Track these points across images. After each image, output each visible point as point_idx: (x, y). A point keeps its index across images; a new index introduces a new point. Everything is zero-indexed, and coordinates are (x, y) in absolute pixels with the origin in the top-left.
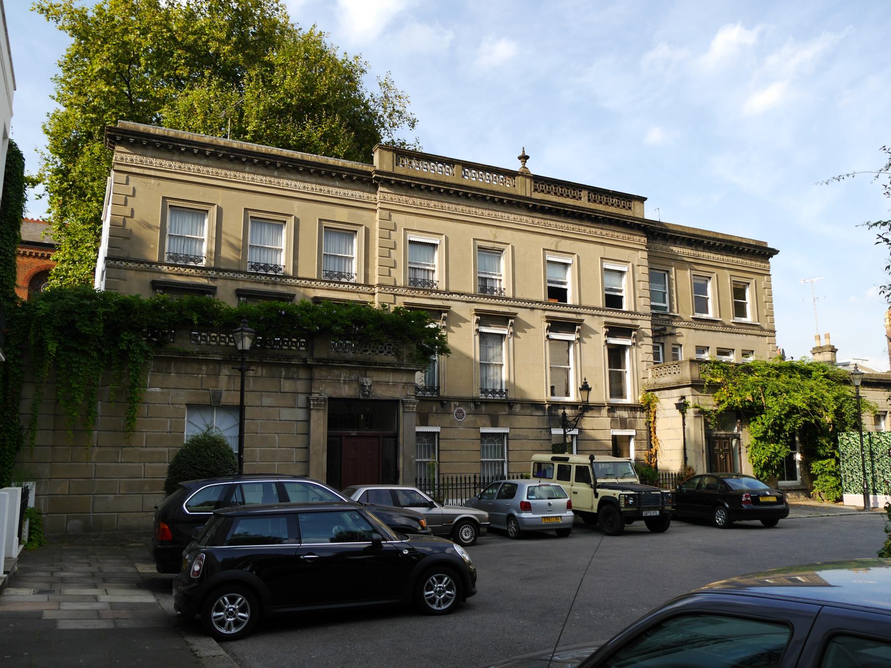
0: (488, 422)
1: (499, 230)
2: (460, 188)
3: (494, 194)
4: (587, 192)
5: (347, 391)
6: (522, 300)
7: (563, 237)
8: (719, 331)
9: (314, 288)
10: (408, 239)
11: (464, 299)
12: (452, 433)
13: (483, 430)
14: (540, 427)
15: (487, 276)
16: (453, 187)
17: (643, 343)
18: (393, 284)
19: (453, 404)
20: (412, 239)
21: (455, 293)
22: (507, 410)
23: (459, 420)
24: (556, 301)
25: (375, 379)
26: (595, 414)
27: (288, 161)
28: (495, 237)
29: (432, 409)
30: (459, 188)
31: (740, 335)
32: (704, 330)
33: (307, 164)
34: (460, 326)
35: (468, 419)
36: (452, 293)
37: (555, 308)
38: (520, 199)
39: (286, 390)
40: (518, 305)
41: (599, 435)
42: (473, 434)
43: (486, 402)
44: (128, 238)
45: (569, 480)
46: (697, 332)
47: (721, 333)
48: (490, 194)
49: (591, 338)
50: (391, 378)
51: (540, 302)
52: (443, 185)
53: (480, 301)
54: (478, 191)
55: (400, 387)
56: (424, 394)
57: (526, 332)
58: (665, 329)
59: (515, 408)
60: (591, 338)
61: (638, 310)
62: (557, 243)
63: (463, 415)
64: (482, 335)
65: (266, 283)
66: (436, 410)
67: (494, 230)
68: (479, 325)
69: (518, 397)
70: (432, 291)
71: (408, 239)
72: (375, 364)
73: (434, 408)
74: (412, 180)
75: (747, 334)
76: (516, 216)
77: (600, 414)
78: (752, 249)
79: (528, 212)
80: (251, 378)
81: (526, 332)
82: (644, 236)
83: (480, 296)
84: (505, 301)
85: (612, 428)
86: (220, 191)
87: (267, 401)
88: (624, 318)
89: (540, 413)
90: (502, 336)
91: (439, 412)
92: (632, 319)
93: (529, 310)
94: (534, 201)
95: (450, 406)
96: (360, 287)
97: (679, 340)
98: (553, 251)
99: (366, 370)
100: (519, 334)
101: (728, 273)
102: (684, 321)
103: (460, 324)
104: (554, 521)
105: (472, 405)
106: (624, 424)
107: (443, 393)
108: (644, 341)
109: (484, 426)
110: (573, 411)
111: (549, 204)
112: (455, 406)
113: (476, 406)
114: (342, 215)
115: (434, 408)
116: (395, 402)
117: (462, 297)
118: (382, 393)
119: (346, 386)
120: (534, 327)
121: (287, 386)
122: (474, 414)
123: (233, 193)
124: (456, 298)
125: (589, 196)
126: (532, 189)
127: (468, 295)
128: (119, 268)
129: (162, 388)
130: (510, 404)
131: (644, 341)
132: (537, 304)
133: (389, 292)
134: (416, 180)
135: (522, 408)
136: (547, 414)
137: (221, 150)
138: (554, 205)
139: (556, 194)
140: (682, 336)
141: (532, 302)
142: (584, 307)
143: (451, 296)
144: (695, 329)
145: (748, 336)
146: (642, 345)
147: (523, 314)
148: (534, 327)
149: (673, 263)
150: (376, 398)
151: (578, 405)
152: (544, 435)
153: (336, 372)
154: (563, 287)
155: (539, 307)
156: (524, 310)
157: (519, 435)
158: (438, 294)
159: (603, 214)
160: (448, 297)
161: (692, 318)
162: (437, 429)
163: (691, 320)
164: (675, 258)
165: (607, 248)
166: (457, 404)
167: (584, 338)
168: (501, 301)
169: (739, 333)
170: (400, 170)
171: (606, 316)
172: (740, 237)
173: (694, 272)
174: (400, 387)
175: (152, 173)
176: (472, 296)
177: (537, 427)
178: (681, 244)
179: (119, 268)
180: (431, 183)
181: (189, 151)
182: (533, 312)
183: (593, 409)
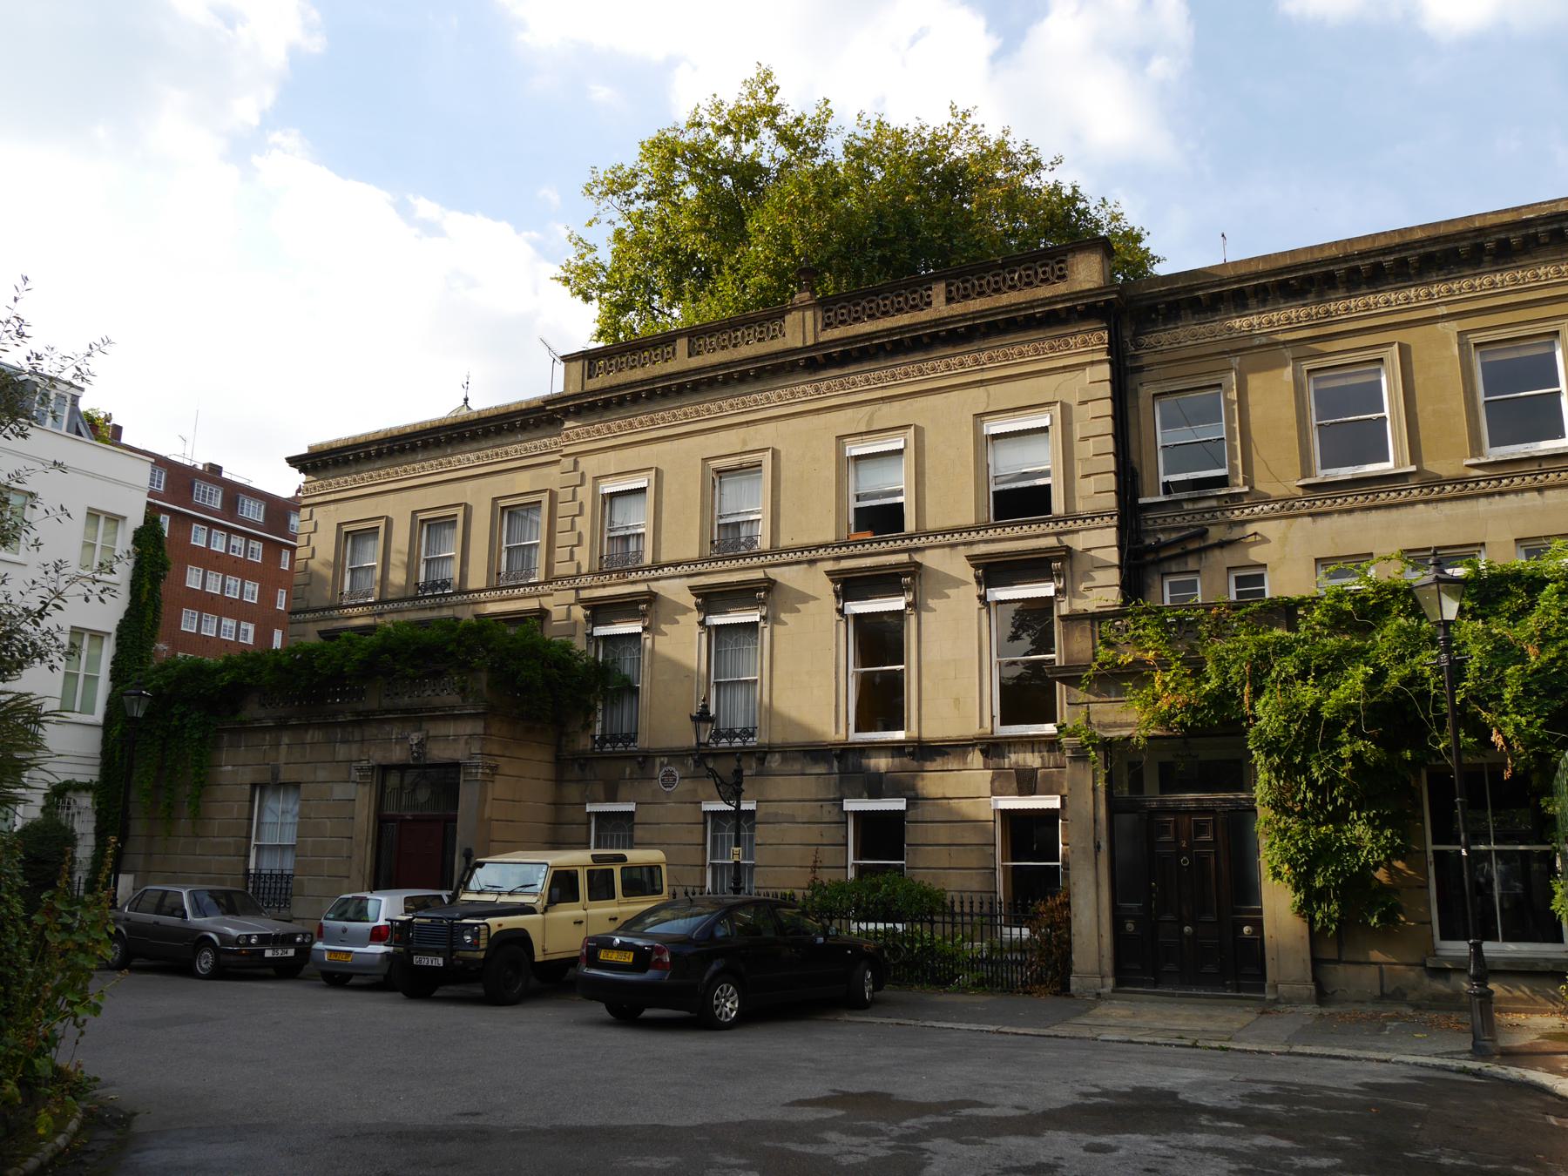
1: (752, 429)
2: (670, 380)
4: (943, 285)
5: (397, 755)
6: (794, 550)
7: (882, 399)
8: (1413, 503)
9: (485, 602)
10: (601, 492)
13: (707, 807)
14: (820, 797)
15: (739, 519)
16: (659, 382)
17: (1089, 584)
18: (574, 572)
19: (658, 761)
20: (607, 491)
22: (754, 765)
23: (668, 789)
24: (868, 535)
25: (432, 733)
27: (450, 430)
28: (744, 443)
30: (667, 380)
31: (1512, 497)
32: (1350, 511)
33: (472, 425)
35: (681, 787)
36: (661, 567)
37: (868, 548)
38: (777, 358)
39: (340, 759)
41: (968, 808)
44: (308, 584)
45: (577, 900)
46: (1324, 523)
47: (1421, 507)
48: (721, 369)
49: (949, 597)
50: (450, 729)
51: (825, 546)
52: (643, 385)
53: (710, 569)
55: (462, 742)
56: (730, 743)
58: (1202, 533)
59: (770, 762)
60: (949, 597)
61: (1081, 507)
62: (872, 414)
63: (675, 780)
64: (710, 630)
65: (431, 609)
66: (631, 773)
67: (743, 431)
68: (708, 613)
69: (778, 739)
70: (630, 571)
71: (601, 492)
72: (436, 709)
75: (1540, 490)
77: (965, 763)
78: (1464, 245)
79: (810, 374)
80: (308, 746)
81: (798, 611)
82: (1101, 329)
83: (716, 560)
84: (755, 559)
85: (994, 793)
86: (391, 496)
87: (322, 775)
88: (1038, 536)
89: (821, 769)
90: (753, 626)
91: (635, 776)
92: (1058, 534)
93: (806, 566)
96: (540, 588)
97: (1256, 554)
98: (861, 434)
99: (421, 720)
100: (783, 616)
101: (1453, 327)
102: (1267, 503)
103: (677, 617)
104: (342, 958)
105: (691, 761)
106: (1027, 783)
107: (643, 742)
108: (1093, 579)
109: (710, 799)
110: (897, 760)
111: (837, 346)
112: (662, 765)
113: (697, 763)
114: (522, 482)
116: (455, 766)
118: (440, 753)
119: (398, 747)
121: (342, 752)
122: (694, 777)
123: (405, 494)
124: (670, 574)
125: (950, 292)
126: (819, 327)
127: (688, 563)
128: (299, 622)
129: (234, 766)
130: (761, 754)
131: (1093, 579)
132: (821, 551)
133: (568, 586)
134: (601, 394)
135: (784, 760)
137: (383, 444)
138: (850, 343)
140: (1265, 540)
141: (809, 548)
142: (927, 534)
143: (660, 571)
144: (1310, 515)
145: (1549, 493)
146: (1090, 589)
147: (782, 575)
149: (1235, 361)
150: (432, 762)
151: (904, 747)
152: (828, 812)
153: (387, 728)
154: (899, 499)
156: (795, 568)
157: (776, 815)
159: (966, 320)
160: (657, 575)
161: (1303, 487)
162: (631, 807)
163: (1300, 492)
164: (1248, 344)
165: (992, 388)
166: (666, 760)
167: (929, 601)
169: (1501, 494)
170: (594, 384)
171: (986, 542)
172: (1506, 211)
173: (1307, 365)
174: (462, 742)
175: (332, 497)
177: (814, 797)
178: (1264, 302)
179: (299, 622)
181: (357, 459)
182: (814, 568)
183: (948, 754)
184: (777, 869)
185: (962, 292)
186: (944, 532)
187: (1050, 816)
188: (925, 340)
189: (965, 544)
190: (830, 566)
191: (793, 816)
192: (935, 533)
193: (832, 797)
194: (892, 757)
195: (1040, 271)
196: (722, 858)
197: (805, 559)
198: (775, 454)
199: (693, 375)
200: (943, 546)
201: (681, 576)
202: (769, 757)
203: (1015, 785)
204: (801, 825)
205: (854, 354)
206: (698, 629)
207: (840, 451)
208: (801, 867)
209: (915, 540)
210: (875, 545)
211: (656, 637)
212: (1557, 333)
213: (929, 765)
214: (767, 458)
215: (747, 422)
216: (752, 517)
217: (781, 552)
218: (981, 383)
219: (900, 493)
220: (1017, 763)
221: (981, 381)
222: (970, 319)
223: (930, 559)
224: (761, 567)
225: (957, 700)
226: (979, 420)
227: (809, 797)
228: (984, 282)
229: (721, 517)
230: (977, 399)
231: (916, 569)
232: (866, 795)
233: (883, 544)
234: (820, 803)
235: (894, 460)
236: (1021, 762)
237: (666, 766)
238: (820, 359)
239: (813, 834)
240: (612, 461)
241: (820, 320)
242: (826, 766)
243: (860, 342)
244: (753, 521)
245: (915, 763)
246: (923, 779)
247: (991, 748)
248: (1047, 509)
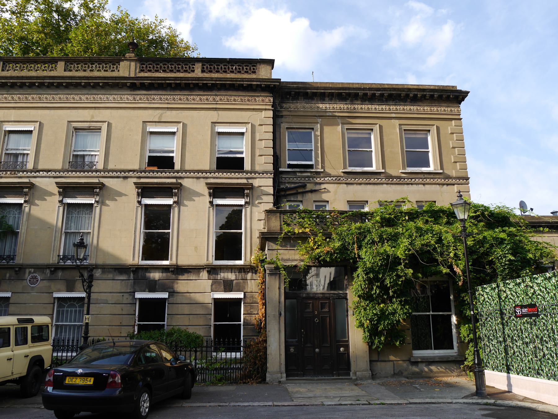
0: (64, 287)
1: (97, 111)
2: (54, 79)
3: (88, 80)
4: (201, 64)
6: (116, 171)
7: (167, 108)
8: (382, 184)
10: (4, 129)
11: (51, 175)
12: (24, 298)
13: (56, 295)
14: (123, 291)
15: (85, 153)
16: (47, 79)
17: (260, 201)
19: (27, 271)
20: (8, 129)
21: (42, 171)
23: (32, 286)
24: (155, 168)
26: (193, 277)
28: (93, 117)
29: (6, 276)
31: (415, 186)
32: (360, 184)
34: (46, 200)
35: (41, 284)
36: (39, 171)
38: (116, 80)
40: (108, 175)
41: (199, 298)
42: (45, 298)
43: (64, 268)
46: (351, 187)
47: (385, 185)
48: (84, 80)
49: (195, 201)
51: (134, 171)
52: (37, 79)
53: (68, 175)
54: (72, 79)
57: (116, 200)
58: (304, 186)
60: (195, 201)
61: (257, 168)
63: (37, 281)
67: (92, 111)
68: (65, 197)
69: (100, 262)
70: (19, 171)
71: (4, 129)
73: (8, 275)
74: (7, 79)
75: (424, 184)
76: (116, 97)
77: (199, 277)
79: (131, 91)
81: (116, 200)
82: (270, 96)
83: (72, 171)
84: (94, 173)
85: (212, 291)
88: (238, 178)
89: (124, 277)
90: (91, 205)
91: (12, 278)
92: (247, 178)
93: (122, 179)
94: (131, 80)
95: (25, 273)
97: (325, 197)
98: (155, 122)
100: (107, 202)
101: (397, 122)
102: (330, 177)
103: (46, 197)
105: (48, 271)
106: (228, 286)
107: (19, 260)
108: (262, 199)
109: (59, 291)
110: (164, 274)
111: (148, 80)
112: (30, 273)
113: (52, 273)
115: (8, 275)
117: (49, 173)
120: (126, 195)
122: (49, 280)
124: (43, 175)
125: (203, 68)
126: (138, 71)
127: (55, 171)
131: (262, 199)
132: (131, 173)
135: (103, 272)
136: (132, 279)
139: (163, 71)
140: (328, 191)
141: (125, 171)
142: (186, 172)
143: (37, 173)
144: (346, 184)
145: (426, 186)
146: (261, 203)
148: (126, 195)
149: (319, 120)
152: (127, 298)
154: (171, 155)
155: (133, 175)
156: (116, 179)
157: (97, 299)
158: (25, 173)
159: (212, 81)
160: (35, 175)
161: (344, 172)
162: (8, 295)
163: (342, 174)
164: (324, 114)
165: (220, 112)
166: (32, 270)
168: (86, 173)
169: (412, 184)
171: (214, 178)
172: (415, 85)
173: (346, 126)
176: (59, 171)
177: (119, 291)
178: (331, 100)
180: (25, 79)
182: (126, 181)
183: (190, 272)
184: (96, 327)
185: (209, 69)
186: (194, 171)
187: (239, 301)
188: (191, 86)
189: (204, 178)
190: (135, 180)
191: (107, 300)
192: (190, 171)
193: (129, 291)
194: (162, 273)
195: (245, 68)
196: (66, 321)
197: (122, 176)
198: (109, 125)
199: (68, 79)
200: (193, 178)
201: (49, 177)
202: (94, 271)
203: (223, 287)
204: (111, 305)
205: (156, 86)
206: (58, 204)
207: (144, 129)
208: (109, 326)
209: (180, 173)
210: (159, 173)
211: (32, 206)
212: (429, 131)
213: (181, 277)
214: (105, 127)
215: (95, 108)
216: (92, 153)
217: (109, 171)
218: (216, 109)
219: (172, 152)
220: (224, 277)
221: (216, 108)
222: (214, 81)
223: (186, 183)
224: (97, 177)
225: (196, 248)
226: (213, 125)
227: (116, 291)
228: (220, 67)
229: (74, 151)
230: (214, 116)
231: (179, 187)
232: (147, 290)
233: (163, 173)
234: (122, 294)
235: (169, 137)
236: (226, 277)
237: (32, 273)
238: (138, 85)
239: (117, 309)
240: (13, 114)
241: (138, 67)
242: (127, 276)
243: (160, 80)
244: (92, 155)
245: (174, 276)
246: (177, 283)
247: (212, 271)
248: (242, 167)
